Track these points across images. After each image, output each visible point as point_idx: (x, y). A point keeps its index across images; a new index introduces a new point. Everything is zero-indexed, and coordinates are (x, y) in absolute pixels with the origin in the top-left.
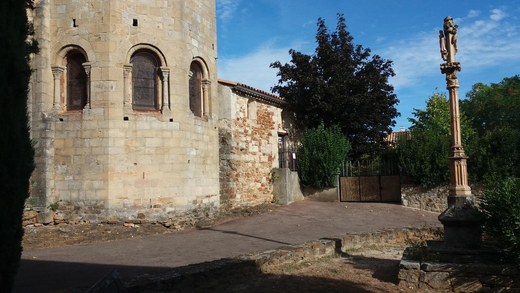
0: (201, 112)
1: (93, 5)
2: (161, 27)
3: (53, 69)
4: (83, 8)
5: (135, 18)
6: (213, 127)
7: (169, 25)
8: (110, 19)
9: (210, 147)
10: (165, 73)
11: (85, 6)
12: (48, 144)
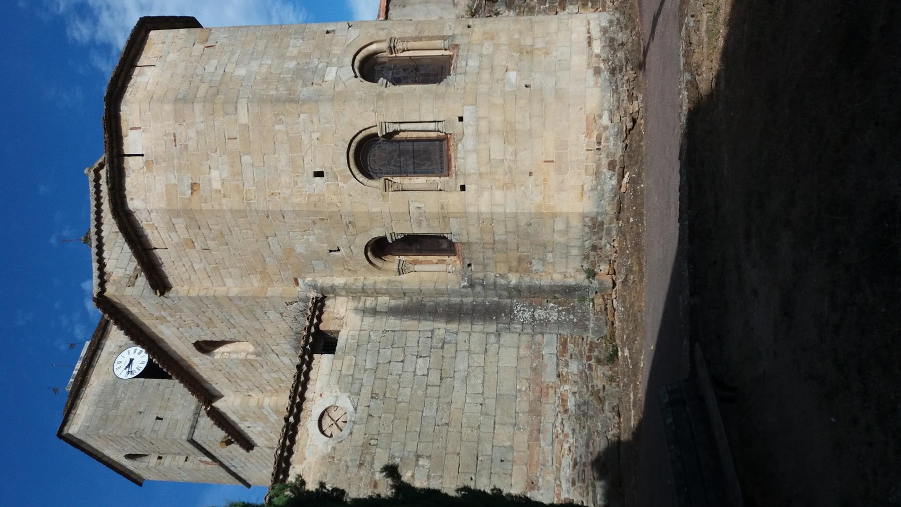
0: (443, 55)
2: (318, 135)
5: (312, 174)
6: (468, 32)
7: (312, 122)
9: (503, 39)
10: (387, 128)
12: (503, 282)
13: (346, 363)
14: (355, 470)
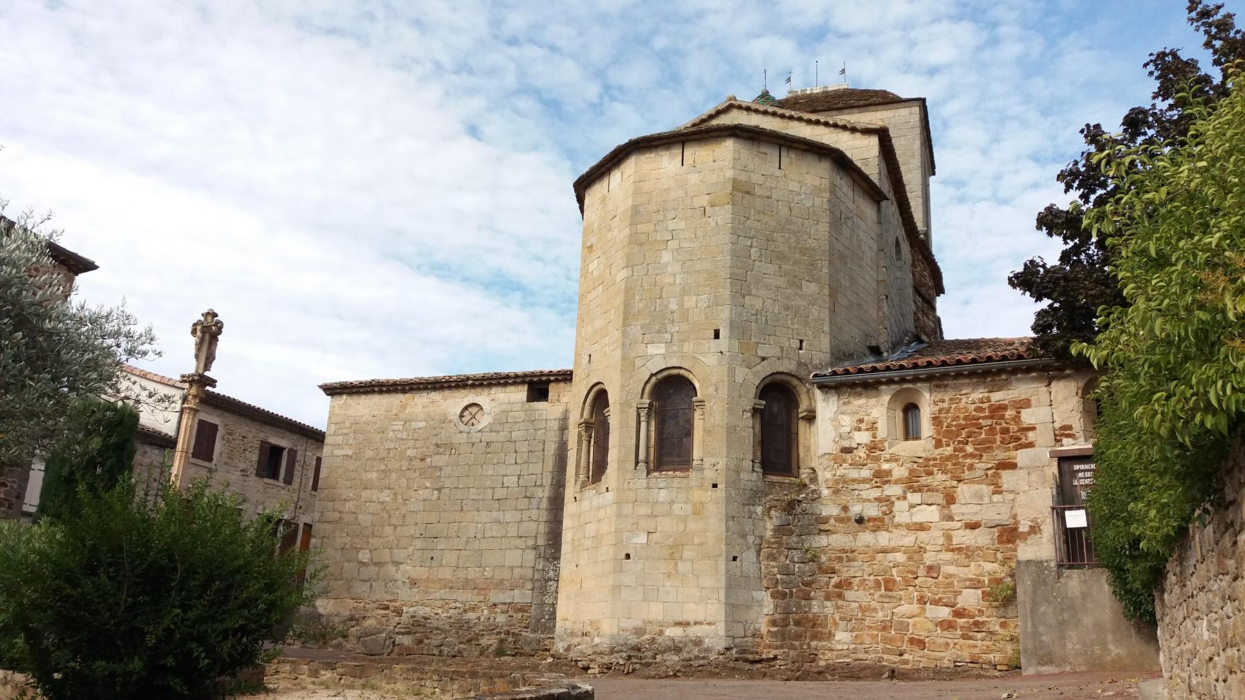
9: (693, 526)
13: (517, 414)
14: (434, 442)
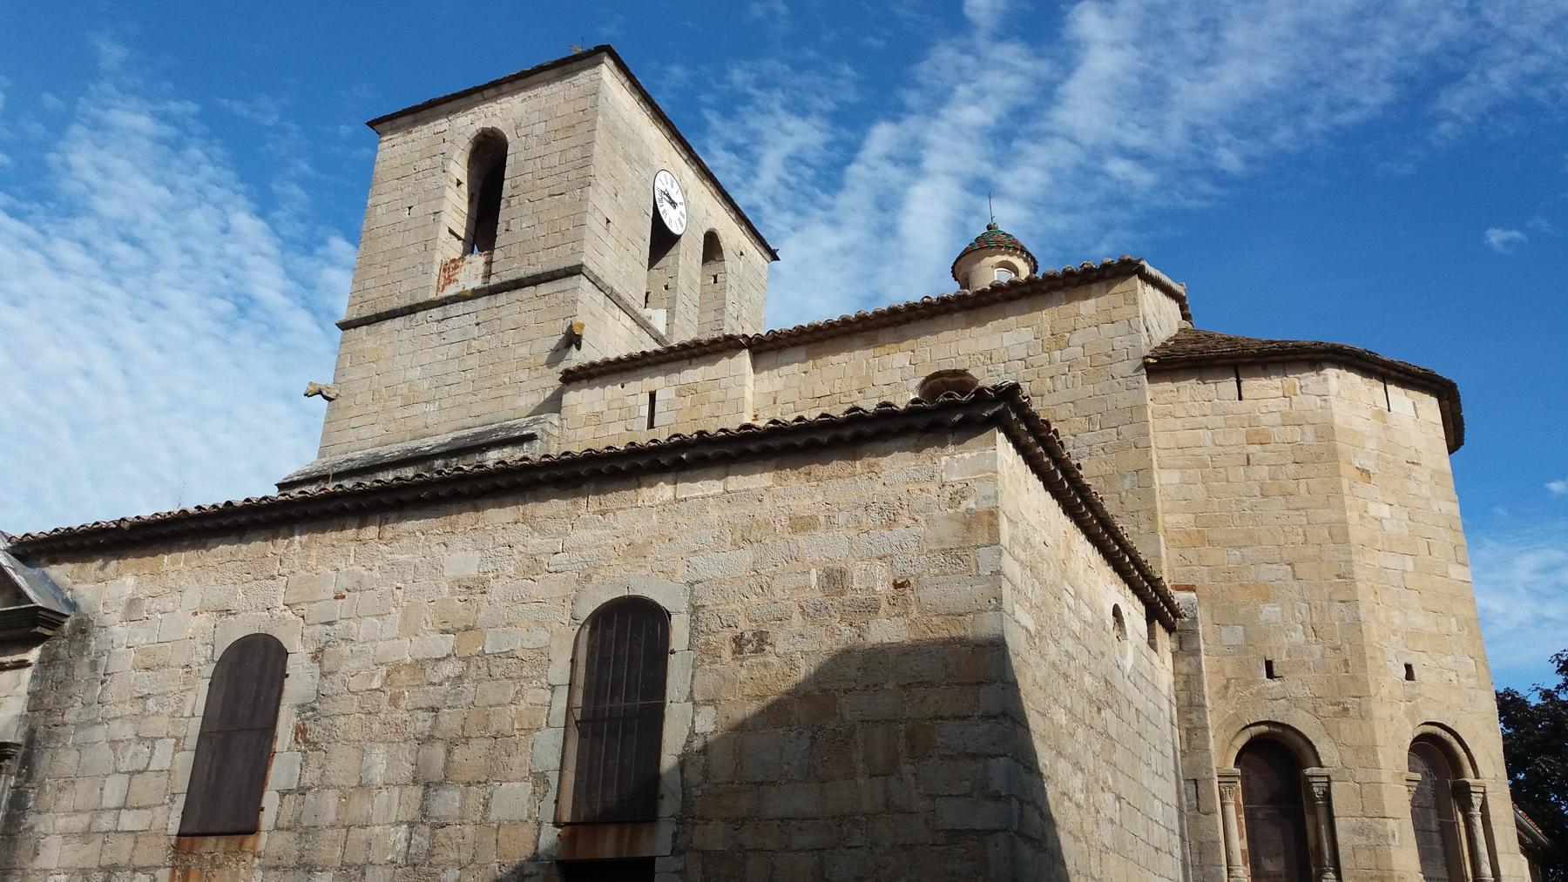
1: (1317, 629)
3: (1222, 779)
4: (1291, 636)
8: (1368, 665)
11: (1295, 630)
